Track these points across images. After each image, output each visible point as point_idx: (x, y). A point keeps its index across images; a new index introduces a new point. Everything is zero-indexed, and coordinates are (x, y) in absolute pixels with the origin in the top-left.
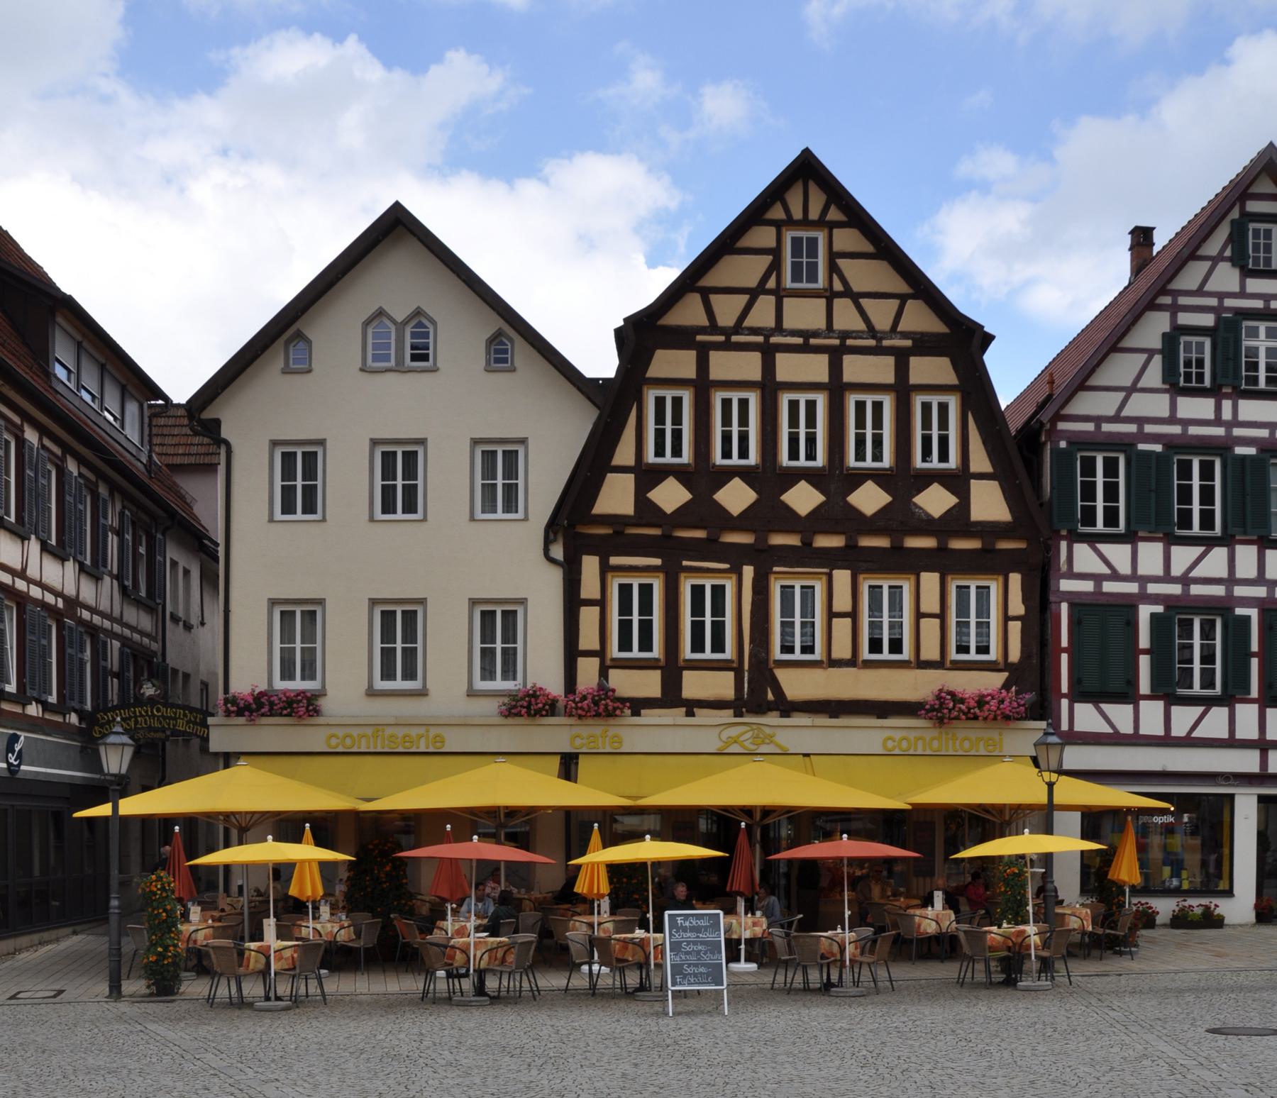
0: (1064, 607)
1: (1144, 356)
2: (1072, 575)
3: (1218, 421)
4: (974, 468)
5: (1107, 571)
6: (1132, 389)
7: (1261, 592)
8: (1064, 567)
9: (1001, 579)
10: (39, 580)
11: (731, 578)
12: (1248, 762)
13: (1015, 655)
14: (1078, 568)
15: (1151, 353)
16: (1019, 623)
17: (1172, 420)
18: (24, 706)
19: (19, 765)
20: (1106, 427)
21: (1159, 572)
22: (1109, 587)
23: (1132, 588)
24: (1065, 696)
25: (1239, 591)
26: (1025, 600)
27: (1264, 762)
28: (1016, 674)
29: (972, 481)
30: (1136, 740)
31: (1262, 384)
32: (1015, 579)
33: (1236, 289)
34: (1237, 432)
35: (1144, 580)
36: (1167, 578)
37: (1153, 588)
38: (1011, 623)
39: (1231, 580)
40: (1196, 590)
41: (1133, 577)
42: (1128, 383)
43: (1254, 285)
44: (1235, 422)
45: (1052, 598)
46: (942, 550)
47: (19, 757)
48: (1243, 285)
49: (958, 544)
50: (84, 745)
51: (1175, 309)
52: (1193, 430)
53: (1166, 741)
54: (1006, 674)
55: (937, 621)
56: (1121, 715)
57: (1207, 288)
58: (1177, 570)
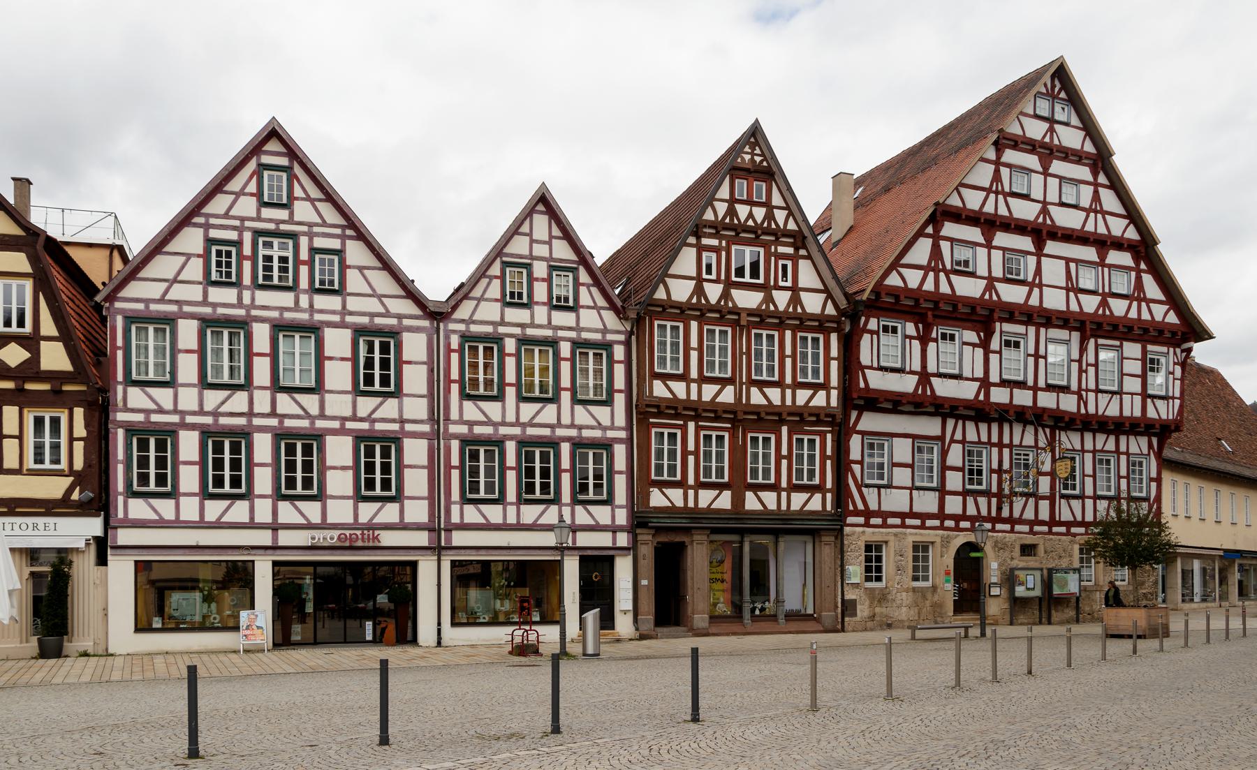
0: (121, 432)
1: (183, 259)
2: (127, 409)
3: (240, 304)
4: (44, 332)
5: (154, 407)
6: (175, 280)
7: (274, 422)
8: (120, 404)
9: (66, 411)
11: (63, 412)
12: (264, 538)
13: (79, 464)
14: (130, 405)
15: (188, 256)
16: (82, 443)
17: (205, 302)
20: (153, 307)
21: (196, 408)
22: (155, 418)
23: (175, 419)
24: (121, 494)
25: (257, 421)
26: (87, 426)
27: (275, 538)
28: (80, 479)
29: (42, 342)
30: (177, 524)
31: (276, 281)
32: (79, 413)
33: (254, 215)
34: (254, 313)
35: (183, 414)
36: (201, 412)
37: (190, 419)
38: (75, 443)
39: (250, 414)
40: (223, 421)
41: (175, 411)
42: (171, 276)
43: (267, 213)
44: (253, 306)
45: (110, 426)
46: (20, 390)
48: (259, 211)
49: (30, 386)
51: (207, 227)
52: (221, 311)
53: (202, 524)
54: (72, 479)
55: (17, 441)
56: (166, 508)
57: (231, 213)
58: (207, 408)
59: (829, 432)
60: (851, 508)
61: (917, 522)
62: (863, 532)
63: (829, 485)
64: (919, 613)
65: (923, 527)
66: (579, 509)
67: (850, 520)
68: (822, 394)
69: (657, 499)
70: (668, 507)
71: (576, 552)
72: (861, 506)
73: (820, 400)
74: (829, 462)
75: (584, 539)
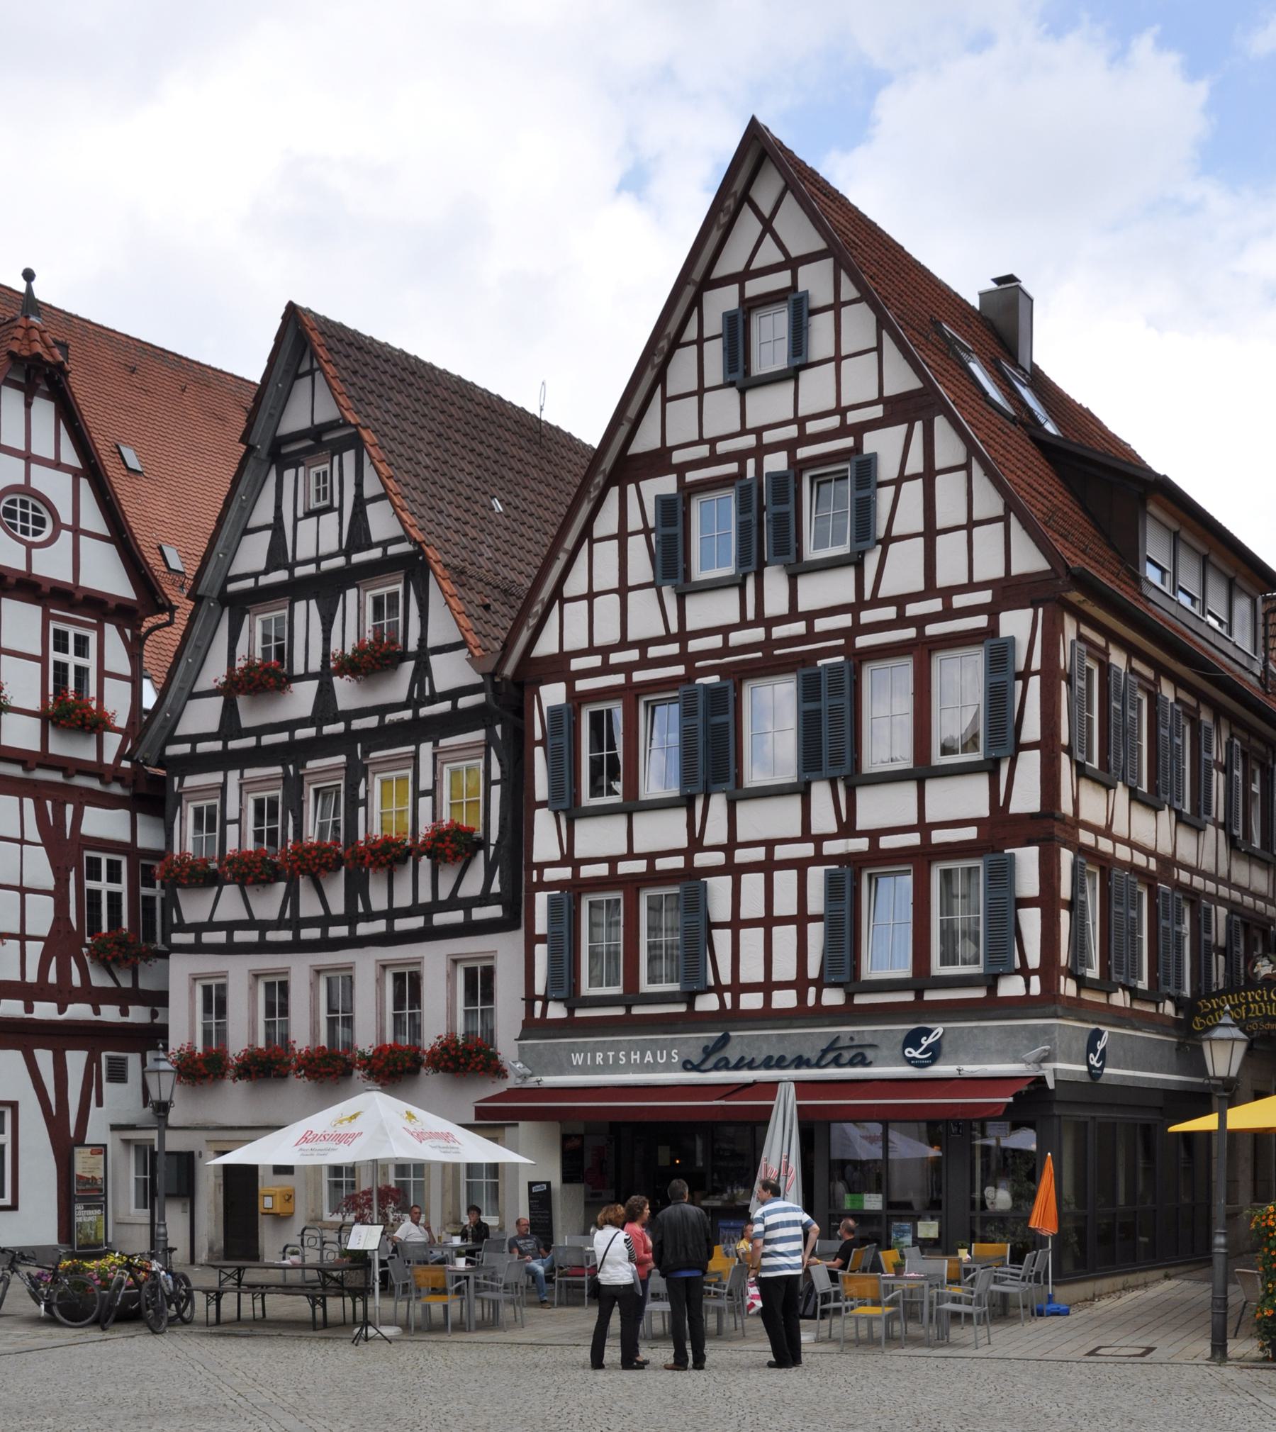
10: (1127, 837)
18: (1108, 994)
19: (1102, 1068)
47: (1102, 1057)
50: (1182, 1040)
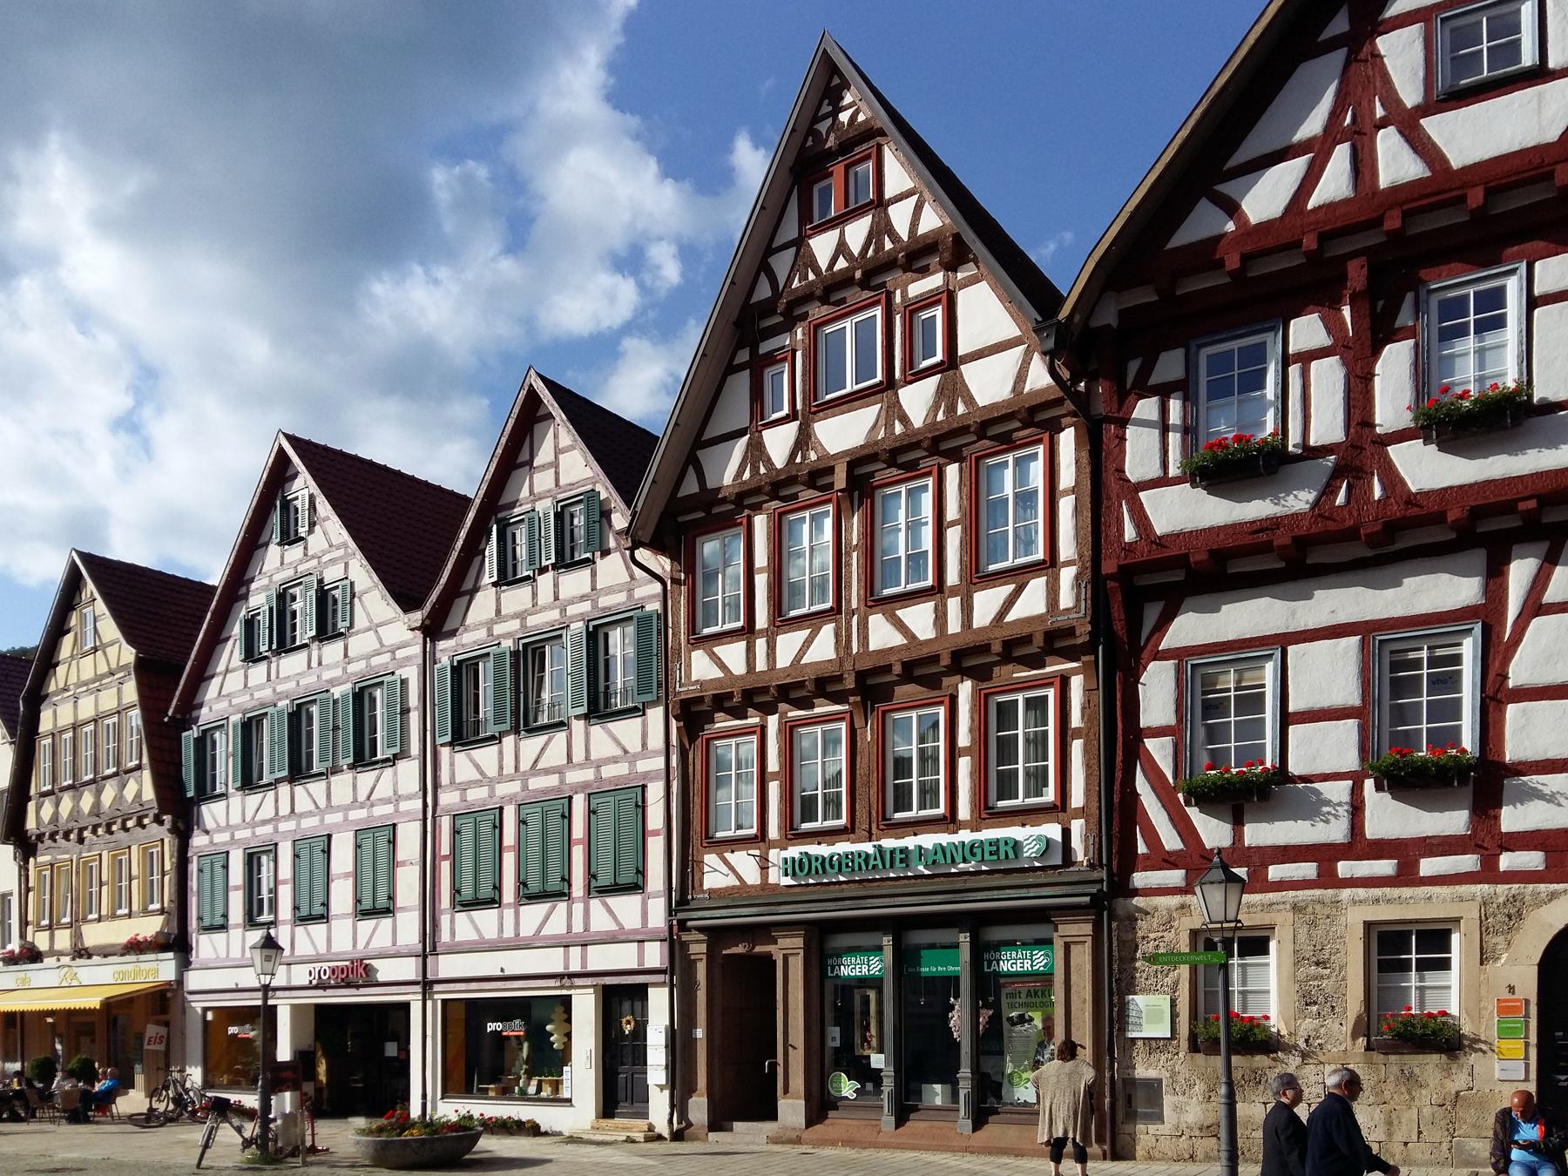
59: (1075, 672)
60: (1142, 848)
61: (1386, 867)
62: (1183, 907)
63: (1077, 798)
64: (1390, 1123)
65: (1407, 876)
66: (595, 904)
67: (1140, 879)
68: (1037, 586)
69: (715, 875)
70: (733, 887)
71: (588, 981)
72: (1171, 840)
73: (1032, 601)
74: (1077, 747)
75: (605, 958)
